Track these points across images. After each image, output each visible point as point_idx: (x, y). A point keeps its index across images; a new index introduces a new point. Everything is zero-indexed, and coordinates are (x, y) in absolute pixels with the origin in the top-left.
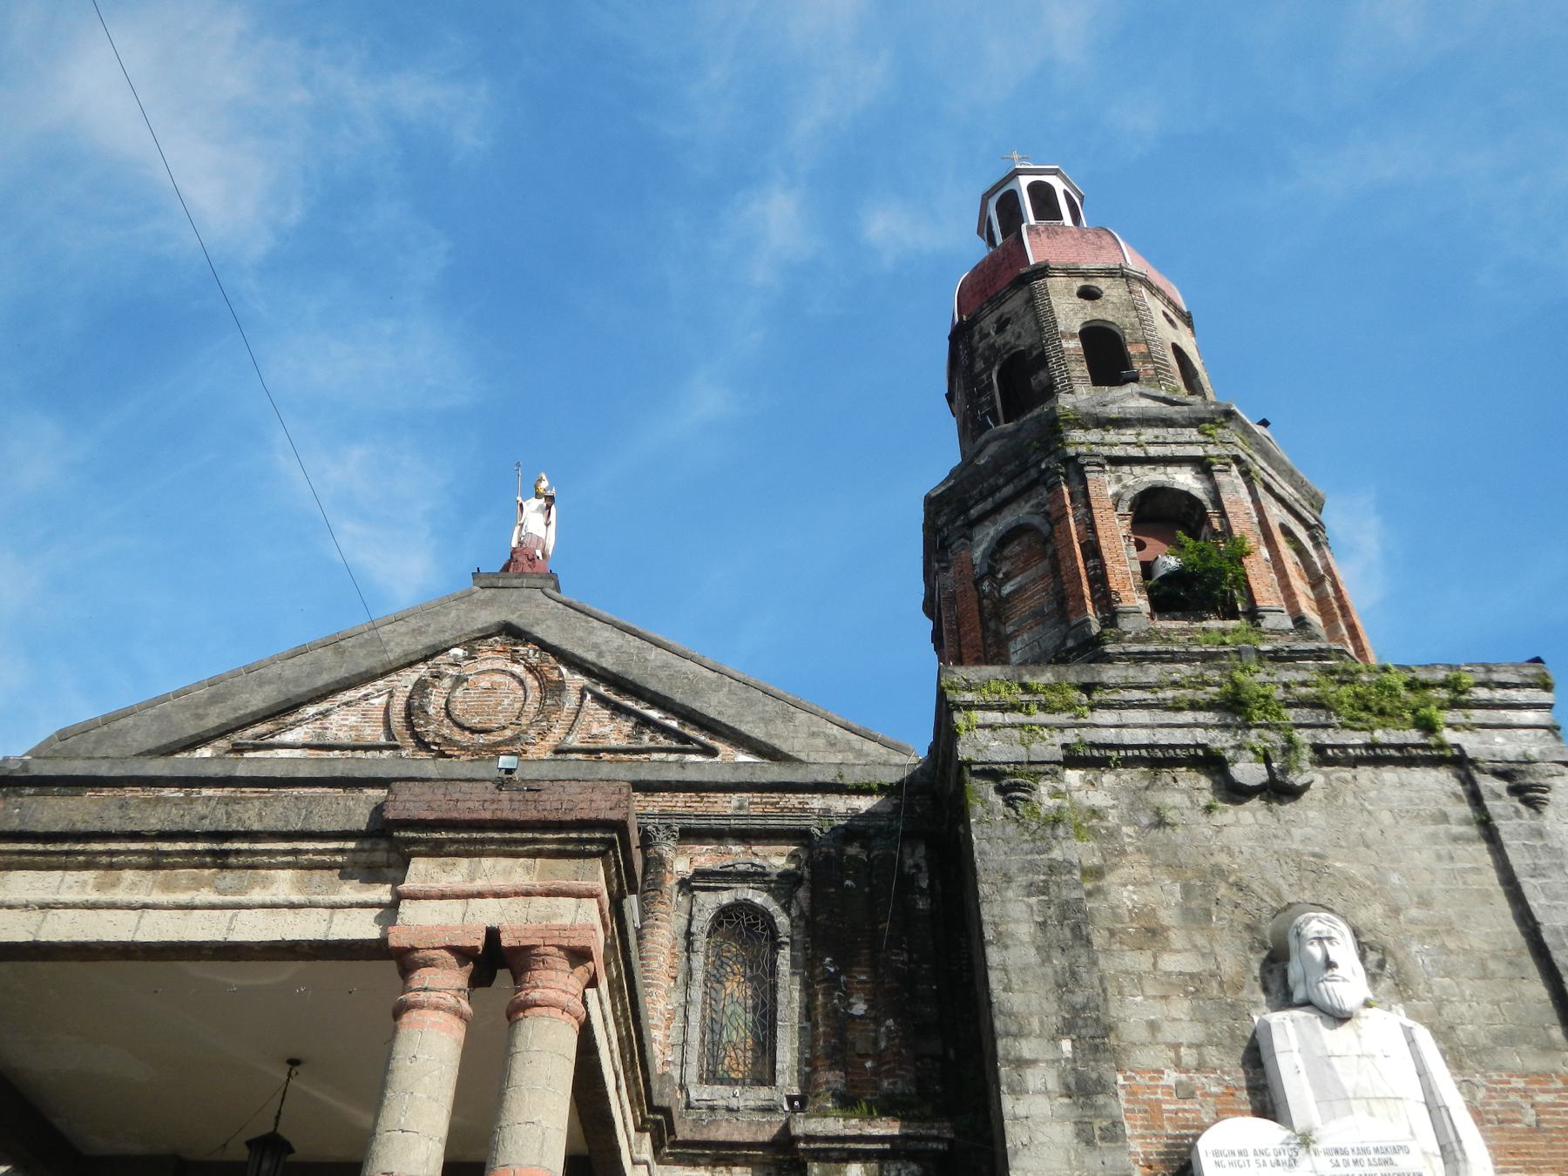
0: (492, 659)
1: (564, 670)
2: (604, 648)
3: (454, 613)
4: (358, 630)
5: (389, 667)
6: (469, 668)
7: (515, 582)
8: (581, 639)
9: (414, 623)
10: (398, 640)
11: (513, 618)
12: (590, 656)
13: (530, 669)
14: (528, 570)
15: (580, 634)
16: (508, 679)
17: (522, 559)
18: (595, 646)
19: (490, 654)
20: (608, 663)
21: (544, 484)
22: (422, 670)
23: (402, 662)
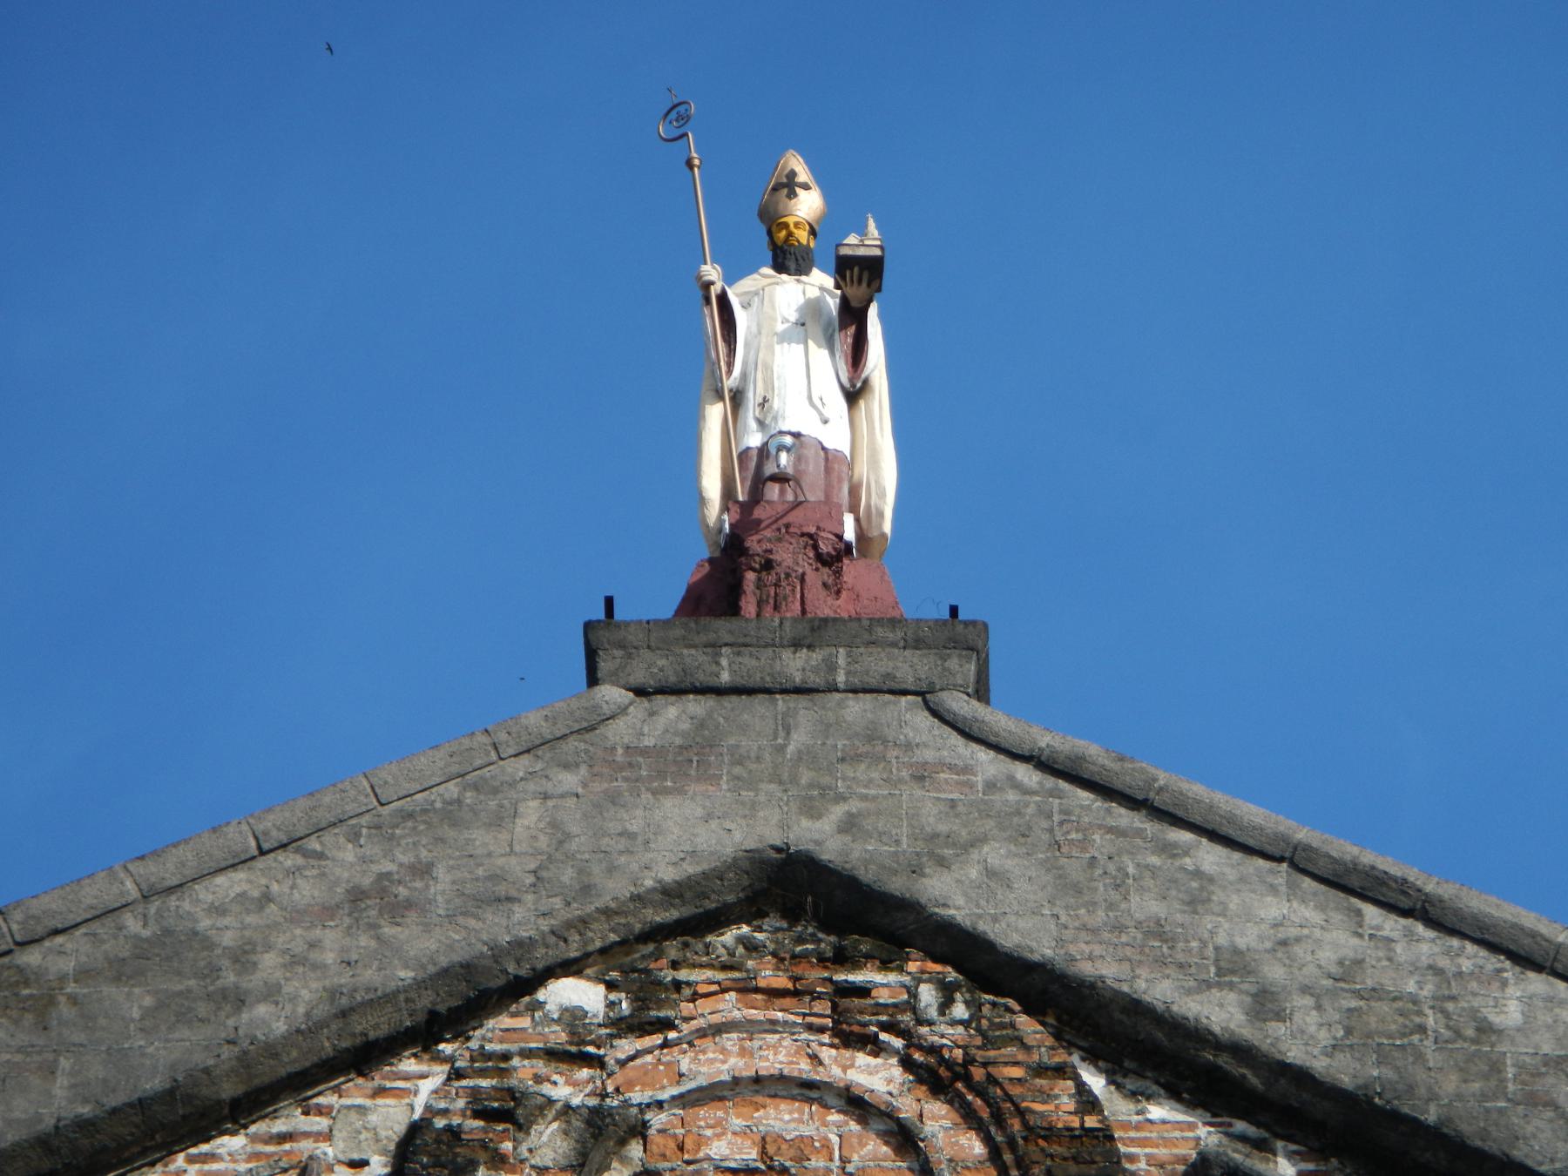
0: (739, 1033)
1: (1096, 1082)
2: (1275, 973)
3: (531, 814)
4: (95, 894)
5: (268, 1072)
6: (646, 1074)
7: (796, 665)
8: (1158, 931)
9: (347, 860)
10: (295, 938)
11: (820, 835)
12: (1221, 1013)
13: (935, 1075)
14: (823, 605)
15: (1146, 905)
16: (834, 1124)
17: (789, 555)
18: (1231, 967)
19: (730, 1006)
20: (1306, 1040)
21: (807, 205)
22: (421, 1087)
23: (326, 1046)
